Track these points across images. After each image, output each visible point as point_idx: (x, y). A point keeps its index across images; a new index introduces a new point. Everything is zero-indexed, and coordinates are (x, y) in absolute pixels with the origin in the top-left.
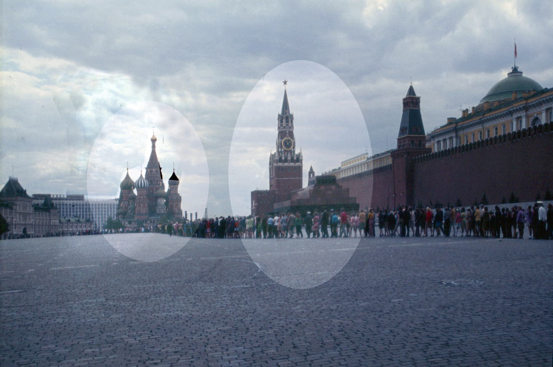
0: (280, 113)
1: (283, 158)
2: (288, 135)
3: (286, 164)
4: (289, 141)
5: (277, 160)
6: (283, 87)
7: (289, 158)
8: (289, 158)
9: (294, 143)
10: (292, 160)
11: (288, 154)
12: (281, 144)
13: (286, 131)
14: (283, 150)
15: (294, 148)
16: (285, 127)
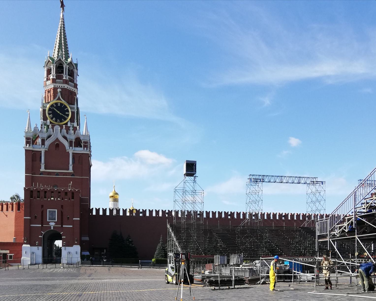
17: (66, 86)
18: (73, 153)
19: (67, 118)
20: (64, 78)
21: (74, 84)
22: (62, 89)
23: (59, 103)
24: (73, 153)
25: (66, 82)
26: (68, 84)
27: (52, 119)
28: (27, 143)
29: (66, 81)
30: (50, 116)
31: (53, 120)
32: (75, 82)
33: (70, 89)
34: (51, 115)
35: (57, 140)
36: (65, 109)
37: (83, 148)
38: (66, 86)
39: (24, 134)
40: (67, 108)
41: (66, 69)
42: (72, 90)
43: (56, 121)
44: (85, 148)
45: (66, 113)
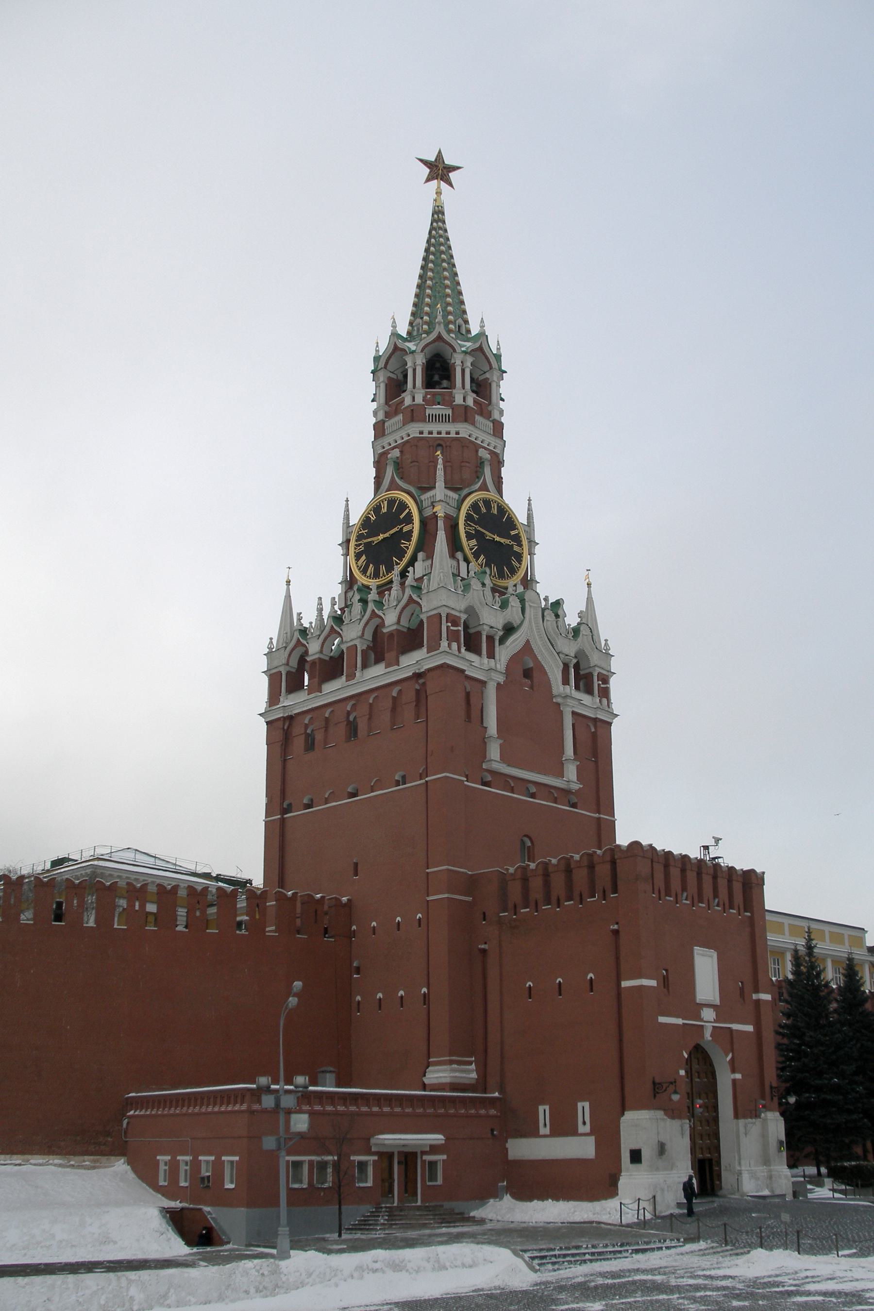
0: (403, 331)
5: (454, 621)
13: (477, 447)
15: (528, 582)
19: (407, 548)
20: (408, 401)
21: (449, 412)
22: (402, 447)
23: (386, 503)
25: (414, 415)
26: (423, 420)
27: (364, 571)
30: (360, 563)
31: (368, 574)
32: (459, 400)
33: (435, 435)
34: (364, 557)
36: (401, 517)
38: (414, 430)
39: (263, 664)
40: (407, 510)
41: (414, 370)
42: (443, 435)
43: (376, 575)
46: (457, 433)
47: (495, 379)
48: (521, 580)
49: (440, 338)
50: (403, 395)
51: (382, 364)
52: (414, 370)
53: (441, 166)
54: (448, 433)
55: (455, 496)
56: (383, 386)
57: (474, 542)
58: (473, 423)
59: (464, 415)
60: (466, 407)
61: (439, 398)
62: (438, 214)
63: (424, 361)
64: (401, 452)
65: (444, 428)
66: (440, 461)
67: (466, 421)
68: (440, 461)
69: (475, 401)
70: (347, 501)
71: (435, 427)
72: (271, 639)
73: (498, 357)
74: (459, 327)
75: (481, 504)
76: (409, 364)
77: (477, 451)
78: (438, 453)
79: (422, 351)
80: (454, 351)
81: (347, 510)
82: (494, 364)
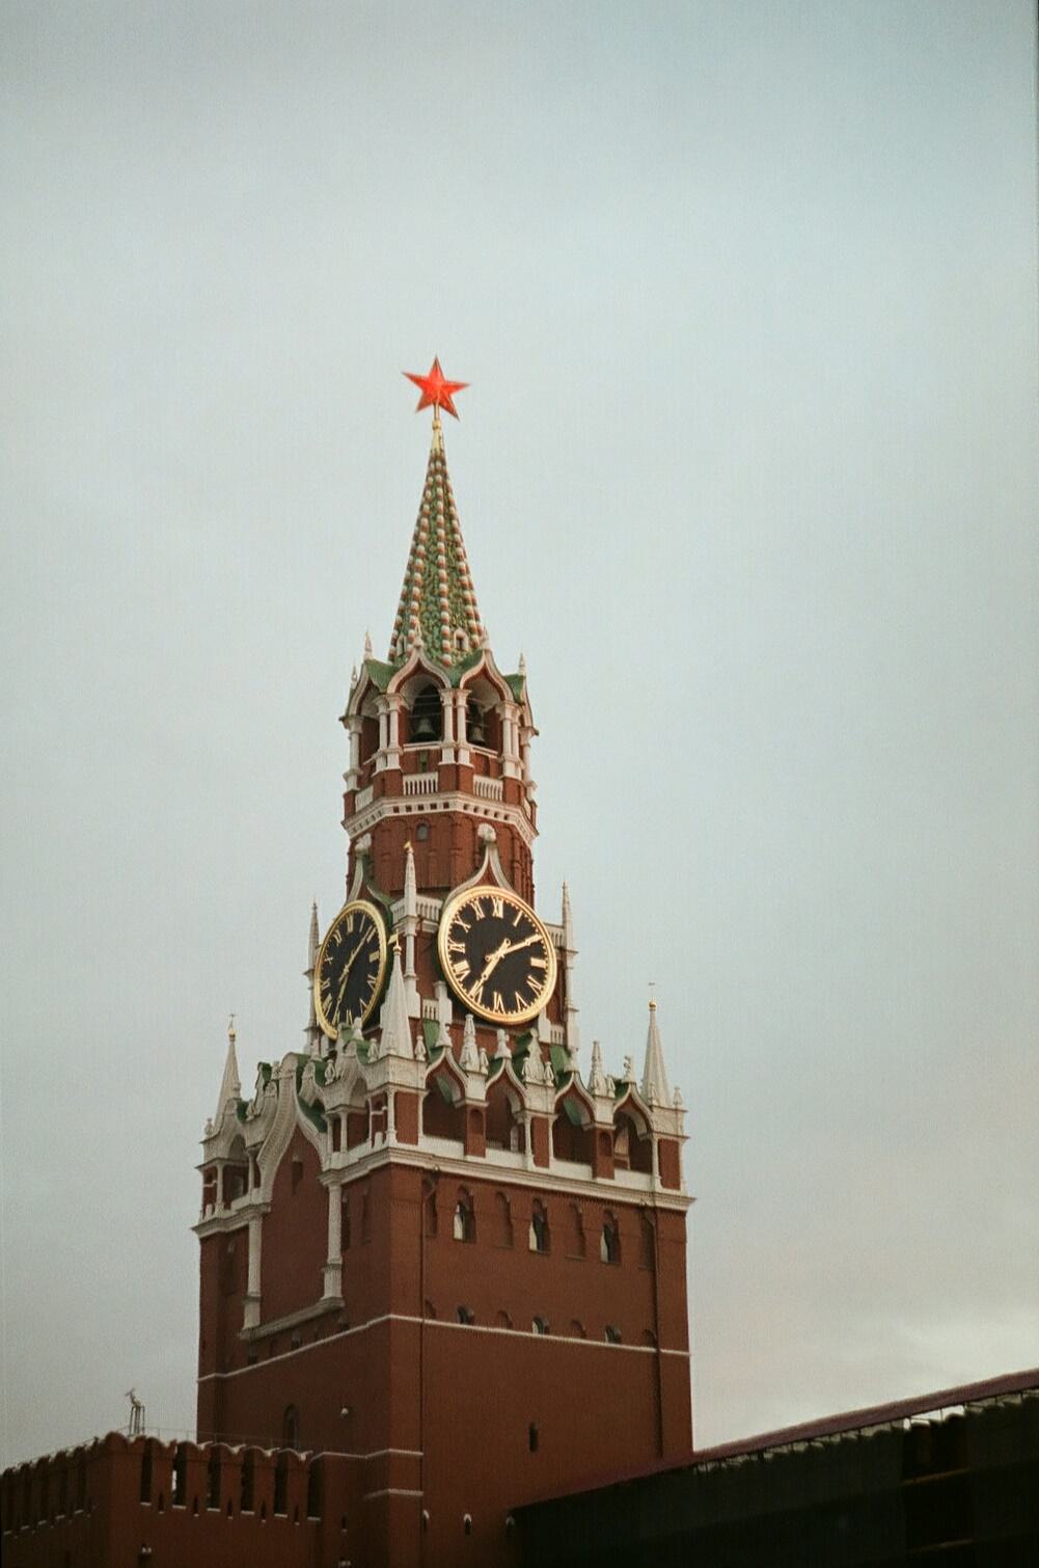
0: (382, 656)
1: (476, 1091)
2: (492, 858)
3: (501, 1163)
4: (516, 926)
5: (404, 1099)
6: (419, 429)
7: (540, 1102)
8: (540, 1102)
9: (562, 968)
10: (574, 1136)
11: (520, 1056)
12: (427, 942)
13: (474, 822)
14: (444, 1010)
15: (559, 1010)
16: (454, 779)
17: (387, 809)
18: (345, 1187)
19: (374, 985)
20: (380, 767)
21: (433, 777)
23: (351, 918)
24: (345, 1187)
25: (386, 786)
27: (330, 1018)
28: (209, 1197)
29: (383, 780)
32: (448, 758)
33: (415, 812)
35: (298, 1131)
37: (369, 1143)
42: (428, 810)
44: (379, 1135)
45: (372, 957)
46: (446, 805)
47: (508, 714)
48: (548, 1006)
49: (419, 667)
50: (374, 756)
51: (354, 711)
52: (388, 717)
53: (439, 384)
54: (434, 806)
55: (437, 903)
56: (355, 738)
57: (463, 965)
58: (470, 791)
59: (454, 779)
60: (457, 768)
61: (423, 759)
62: (437, 458)
63: (403, 703)
64: (373, 838)
65: (427, 802)
66: (411, 857)
67: (457, 788)
68: (411, 857)
69: (475, 757)
70: (315, 908)
71: (414, 803)
72: (209, 1120)
73: (516, 681)
74: (460, 639)
75: (477, 907)
76: (382, 709)
77: (475, 830)
78: (408, 845)
79: (398, 689)
80: (444, 686)
81: (315, 925)
82: (509, 696)
